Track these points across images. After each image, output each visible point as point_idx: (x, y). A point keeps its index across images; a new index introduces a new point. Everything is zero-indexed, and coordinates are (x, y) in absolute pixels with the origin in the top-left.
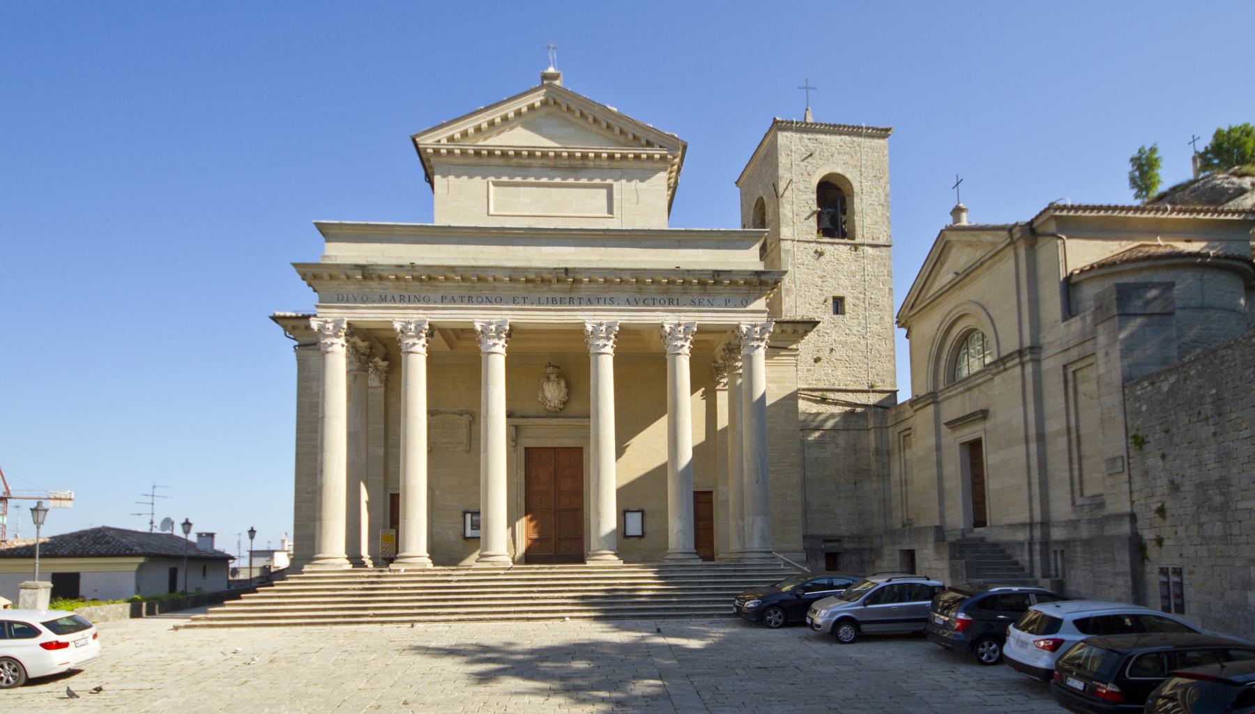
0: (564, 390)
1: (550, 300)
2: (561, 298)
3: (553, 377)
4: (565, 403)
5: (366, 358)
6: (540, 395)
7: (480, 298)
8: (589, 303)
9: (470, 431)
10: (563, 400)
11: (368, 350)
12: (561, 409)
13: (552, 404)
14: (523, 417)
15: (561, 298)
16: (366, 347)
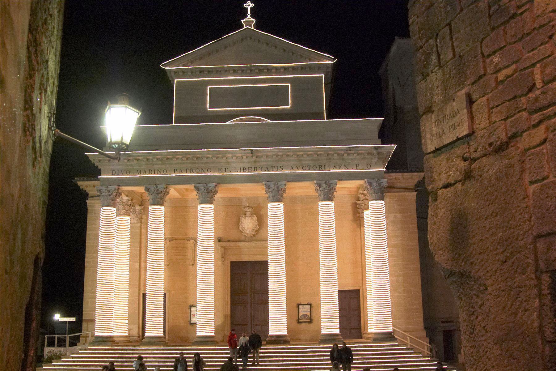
0: (257, 223)
1: (242, 169)
2: (249, 168)
3: (248, 214)
4: (257, 231)
5: (128, 207)
6: (240, 226)
7: (198, 170)
8: (267, 170)
9: (194, 251)
10: (256, 229)
11: (130, 202)
12: (254, 236)
13: (248, 232)
14: (229, 241)
15: (249, 168)
16: (128, 200)
